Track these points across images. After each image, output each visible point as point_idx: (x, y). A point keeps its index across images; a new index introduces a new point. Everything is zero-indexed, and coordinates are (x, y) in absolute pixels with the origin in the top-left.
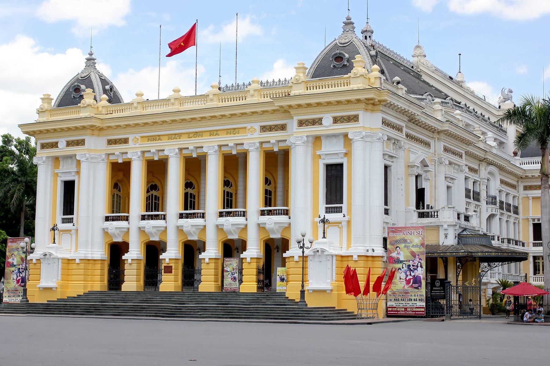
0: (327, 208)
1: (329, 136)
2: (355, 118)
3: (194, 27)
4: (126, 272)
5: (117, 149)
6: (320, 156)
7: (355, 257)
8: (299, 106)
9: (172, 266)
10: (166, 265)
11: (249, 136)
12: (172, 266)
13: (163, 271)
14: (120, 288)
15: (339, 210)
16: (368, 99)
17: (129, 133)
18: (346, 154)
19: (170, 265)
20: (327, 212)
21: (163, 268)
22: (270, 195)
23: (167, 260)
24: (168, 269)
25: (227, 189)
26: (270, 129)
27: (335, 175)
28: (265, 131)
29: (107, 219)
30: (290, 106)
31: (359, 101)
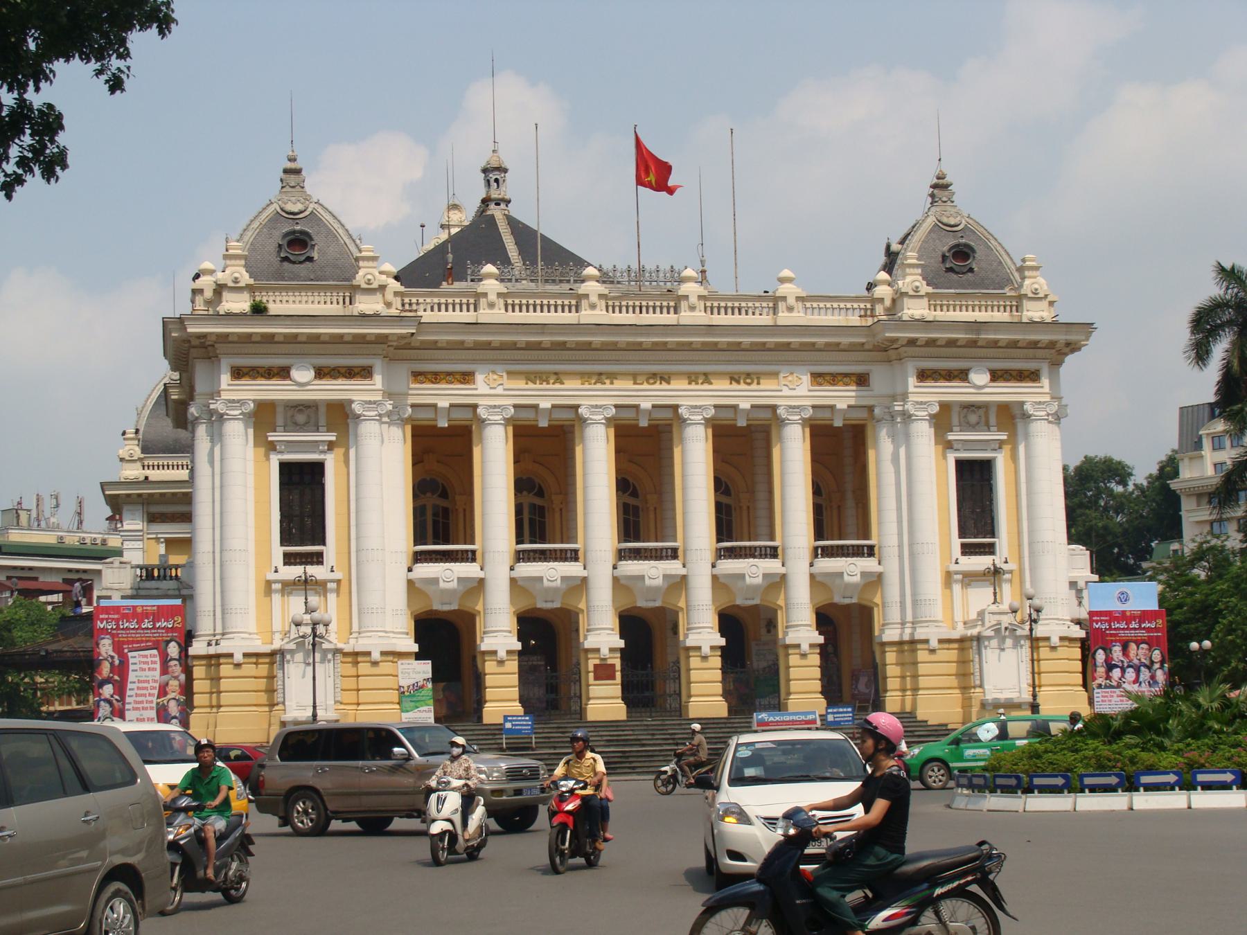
0: (963, 546)
1: (969, 407)
2: (1034, 376)
3: (638, 144)
4: (489, 680)
5: (443, 396)
6: (950, 441)
7: (1055, 640)
8: (931, 343)
9: (613, 666)
10: (597, 662)
11: (786, 392)
12: (613, 666)
13: (591, 675)
14: (480, 718)
15: (989, 549)
16: (1068, 344)
17: (474, 361)
18: (1001, 444)
19: (610, 662)
20: (964, 553)
21: (591, 668)
22: (729, 513)
23: (605, 652)
24: (604, 672)
25: (724, 500)
26: (834, 379)
27: (975, 480)
28: (821, 385)
29: (419, 557)
30: (912, 342)
31: (1052, 345)
